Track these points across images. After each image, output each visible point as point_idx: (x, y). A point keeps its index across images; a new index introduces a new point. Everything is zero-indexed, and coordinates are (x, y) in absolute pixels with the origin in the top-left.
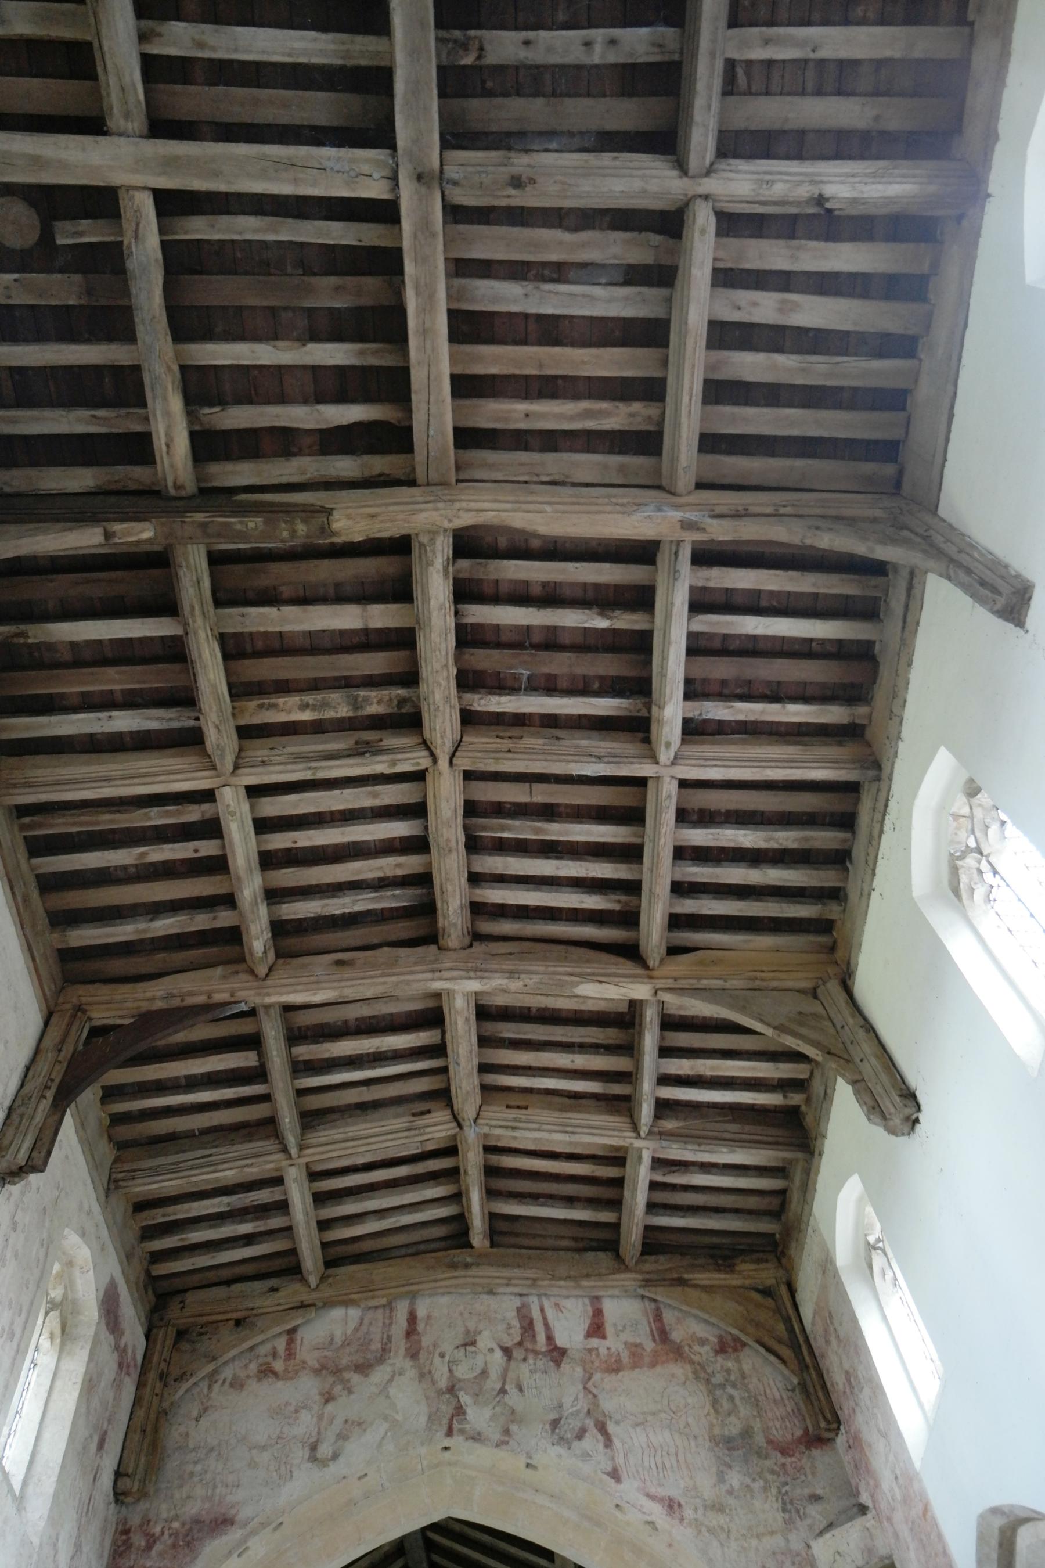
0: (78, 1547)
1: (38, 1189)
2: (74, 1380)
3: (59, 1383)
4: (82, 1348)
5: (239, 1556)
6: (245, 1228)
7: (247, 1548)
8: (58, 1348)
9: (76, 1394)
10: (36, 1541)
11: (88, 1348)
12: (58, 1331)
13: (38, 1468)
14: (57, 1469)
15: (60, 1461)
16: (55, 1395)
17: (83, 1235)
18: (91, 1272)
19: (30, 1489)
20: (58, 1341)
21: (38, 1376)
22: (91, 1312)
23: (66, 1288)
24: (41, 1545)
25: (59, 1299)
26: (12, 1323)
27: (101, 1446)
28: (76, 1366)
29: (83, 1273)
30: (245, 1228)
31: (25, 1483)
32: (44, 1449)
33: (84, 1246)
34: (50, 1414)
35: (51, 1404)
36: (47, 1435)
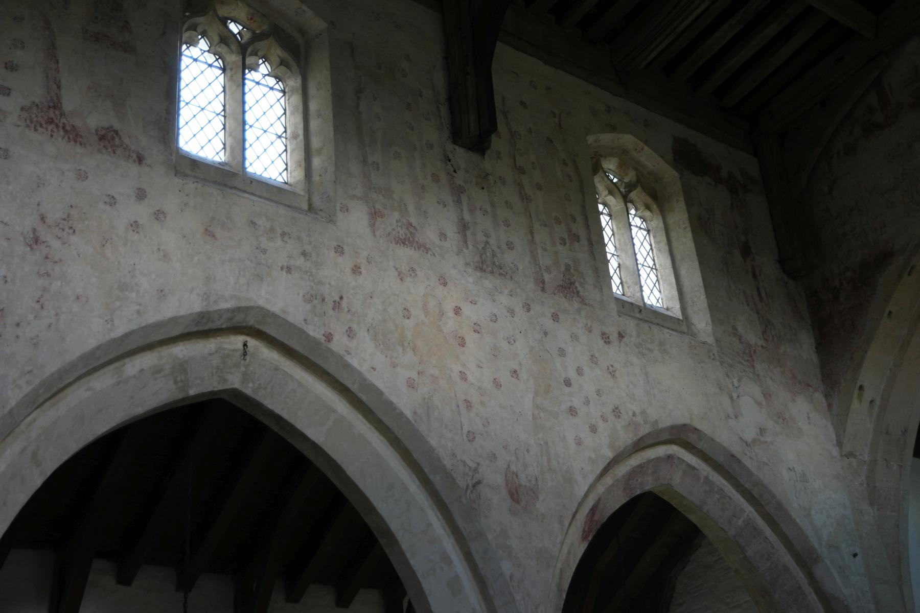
0: (766, 325)
1: (530, 131)
2: (684, 226)
3: (673, 234)
4: (677, 201)
5: (909, 274)
6: (772, 30)
7: (913, 268)
8: (658, 211)
9: (690, 235)
10: (711, 340)
11: (682, 199)
12: (649, 200)
13: (688, 297)
14: (703, 290)
15: (702, 284)
16: (675, 244)
17: (613, 129)
18: (646, 148)
19: (690, 311)
20: (655, 207)
21: (654, 237)
22: (670, 174)
23: (635, 169)
24: (717, 340)
25: (634, 179)
26: (569, 231)
27: (746, 252)
28: (680, 215)
29: (640, 152)
30: (772, 30)
31: (683, 308)
32: (687, 284)
33: (621, 135)
34: (678, 257)
35: (675, 251)
36: (683, 272)
